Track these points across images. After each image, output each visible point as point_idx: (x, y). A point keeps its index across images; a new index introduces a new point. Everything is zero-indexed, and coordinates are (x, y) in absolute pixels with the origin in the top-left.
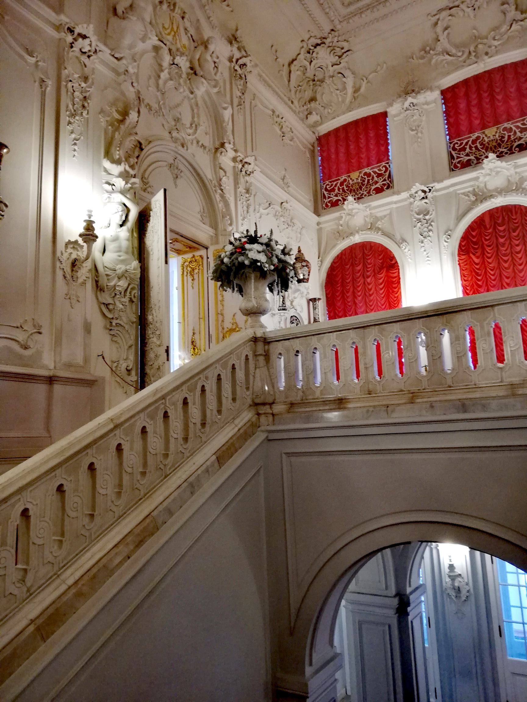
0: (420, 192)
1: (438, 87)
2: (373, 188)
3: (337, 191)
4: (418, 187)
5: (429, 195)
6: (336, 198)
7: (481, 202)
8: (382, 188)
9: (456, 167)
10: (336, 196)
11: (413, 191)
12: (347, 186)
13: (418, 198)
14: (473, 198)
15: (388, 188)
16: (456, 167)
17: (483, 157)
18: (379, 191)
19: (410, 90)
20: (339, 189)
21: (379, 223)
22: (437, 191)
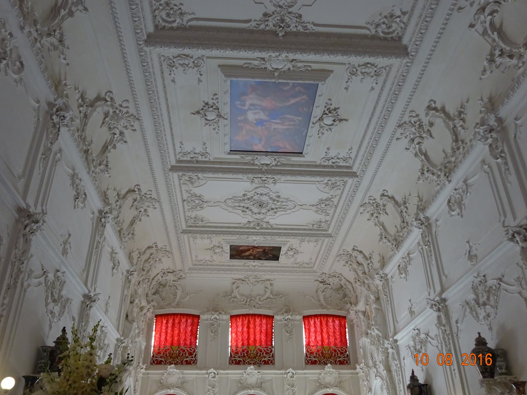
0: (212, 374)
1: (229, 313)
2: (185, 360)
3: (162, 354)
4: (212, 370)
5: (217, 376)
6: (161, 359)
7: (243, 389)
8: (190, 362)
9: (233, 363)
10: (161, 357)
11: (209, 371)
12: (169, 354)
13: (210, 376)
14: (240, 385)
15: (193, 363)
16: (233, 363)
17: (247, 361)
18: (188, 363)
19: (216, 310)
20: (164, 354)
21: (185, 384)
22: (221, 374)
